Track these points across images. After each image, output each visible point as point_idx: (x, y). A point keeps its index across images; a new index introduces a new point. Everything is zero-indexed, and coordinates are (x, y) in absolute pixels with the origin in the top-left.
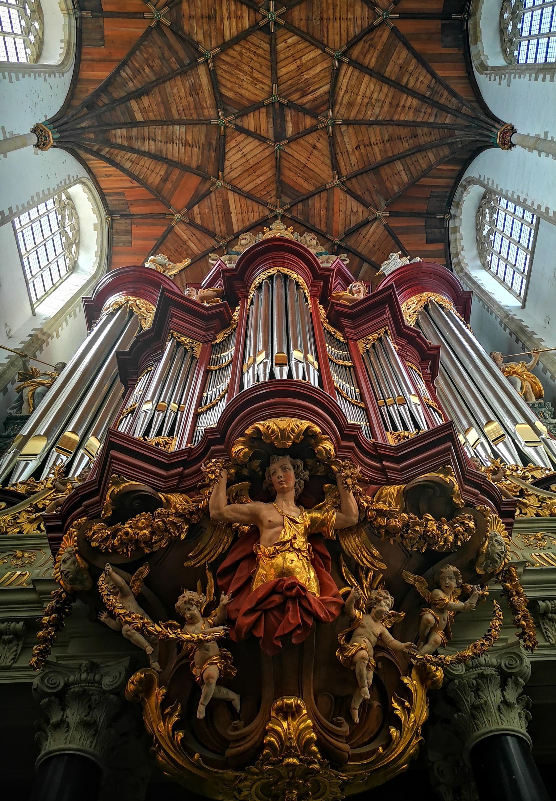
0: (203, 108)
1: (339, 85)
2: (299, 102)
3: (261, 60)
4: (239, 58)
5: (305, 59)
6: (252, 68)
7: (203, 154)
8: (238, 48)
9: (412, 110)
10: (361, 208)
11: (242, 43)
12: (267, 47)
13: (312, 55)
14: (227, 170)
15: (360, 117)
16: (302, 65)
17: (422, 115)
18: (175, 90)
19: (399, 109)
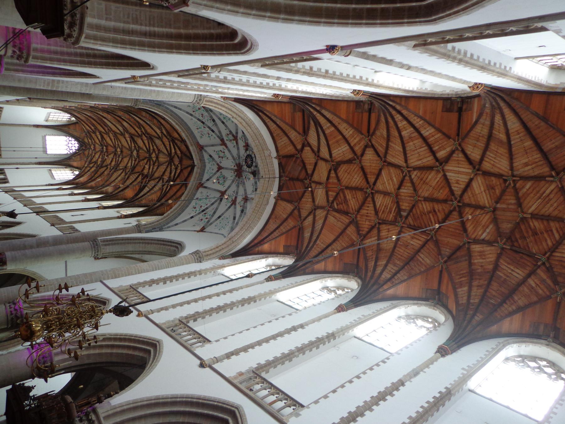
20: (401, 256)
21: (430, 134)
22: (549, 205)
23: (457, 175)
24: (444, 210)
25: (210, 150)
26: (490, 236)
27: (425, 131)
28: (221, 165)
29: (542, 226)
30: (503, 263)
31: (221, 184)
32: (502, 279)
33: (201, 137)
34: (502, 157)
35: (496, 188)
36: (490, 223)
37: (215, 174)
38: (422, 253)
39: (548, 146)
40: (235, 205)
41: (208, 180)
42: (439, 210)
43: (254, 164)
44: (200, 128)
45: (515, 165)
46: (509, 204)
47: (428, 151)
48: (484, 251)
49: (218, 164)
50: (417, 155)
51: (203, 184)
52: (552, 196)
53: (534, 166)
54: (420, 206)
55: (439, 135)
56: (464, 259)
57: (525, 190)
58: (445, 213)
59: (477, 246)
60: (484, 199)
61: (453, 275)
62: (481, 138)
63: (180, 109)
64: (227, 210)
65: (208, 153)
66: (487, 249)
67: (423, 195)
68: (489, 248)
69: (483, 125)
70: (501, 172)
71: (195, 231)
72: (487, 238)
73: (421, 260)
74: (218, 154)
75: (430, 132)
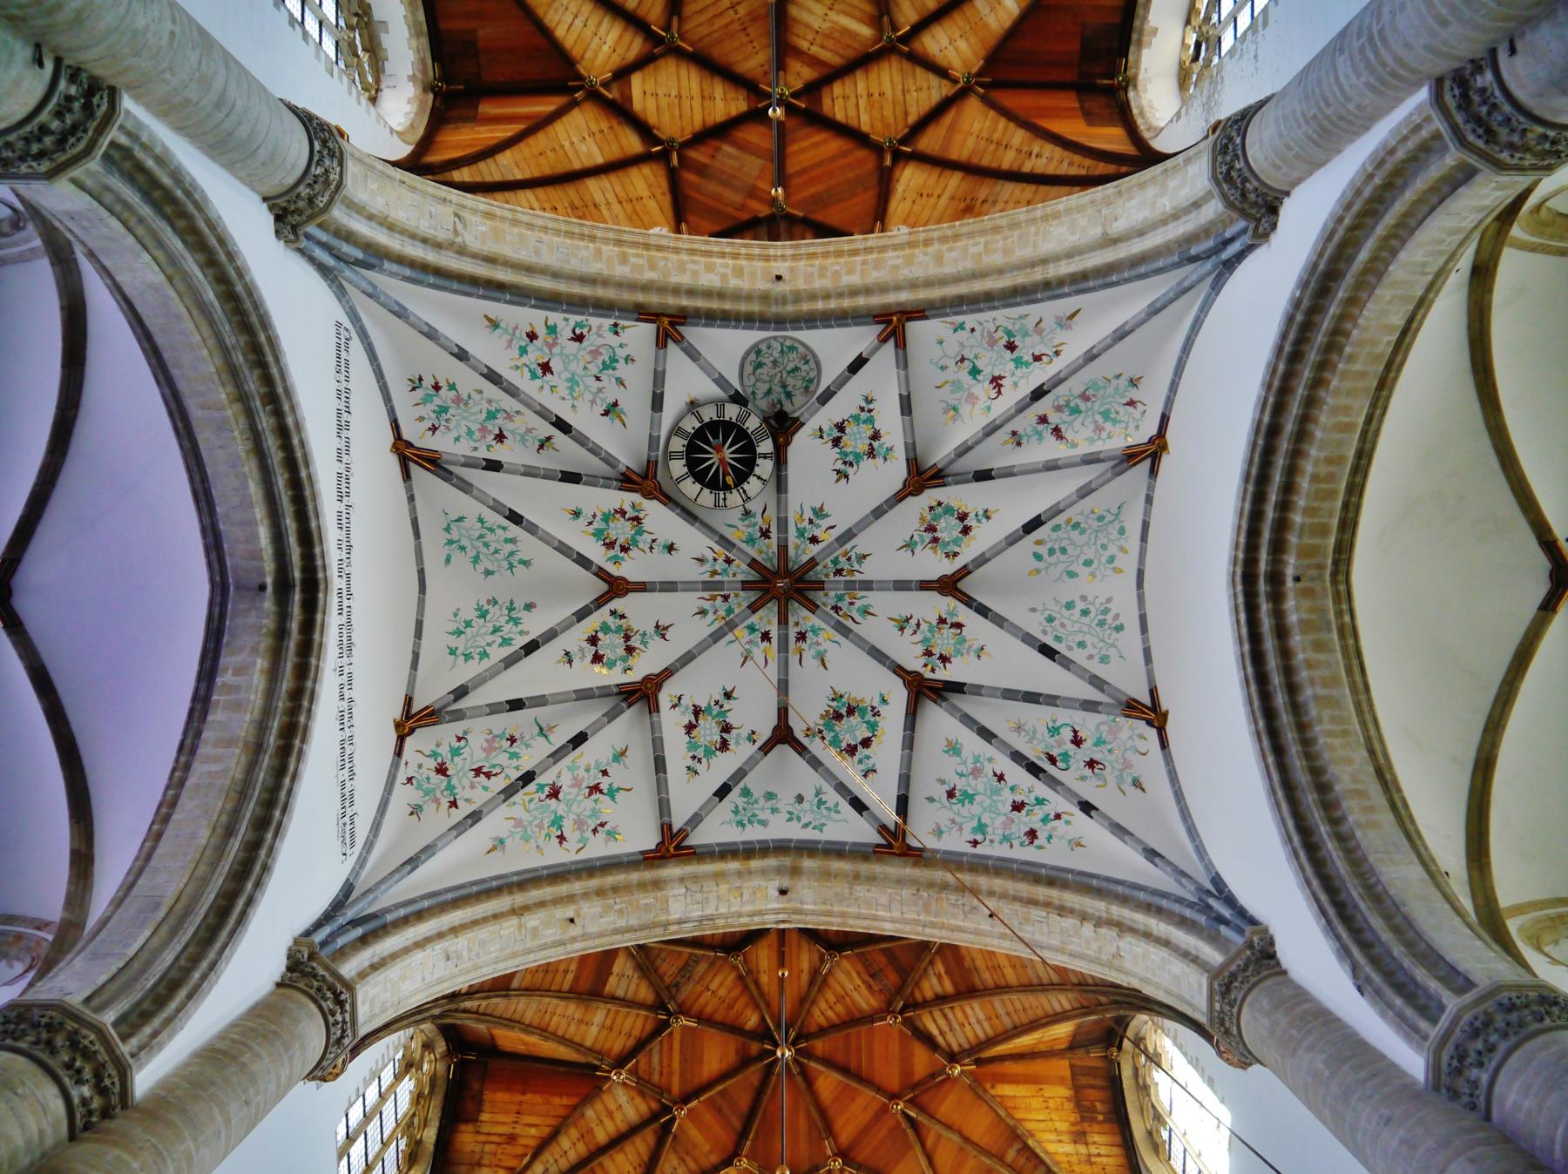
25: (687, 796)
28: (765, 733)
31: (873, 727)
33: (611, 835)
37: (815, 763)
40: (964, 572)
41: (859, 805)
43: (732, 412)
44: (557, 822)
49: (766, 748)
51: (882, 829)
63: (429, 850)
64: (999, 621)
65: (707, 808)
71: (1164, 744)
74: (709, 753)
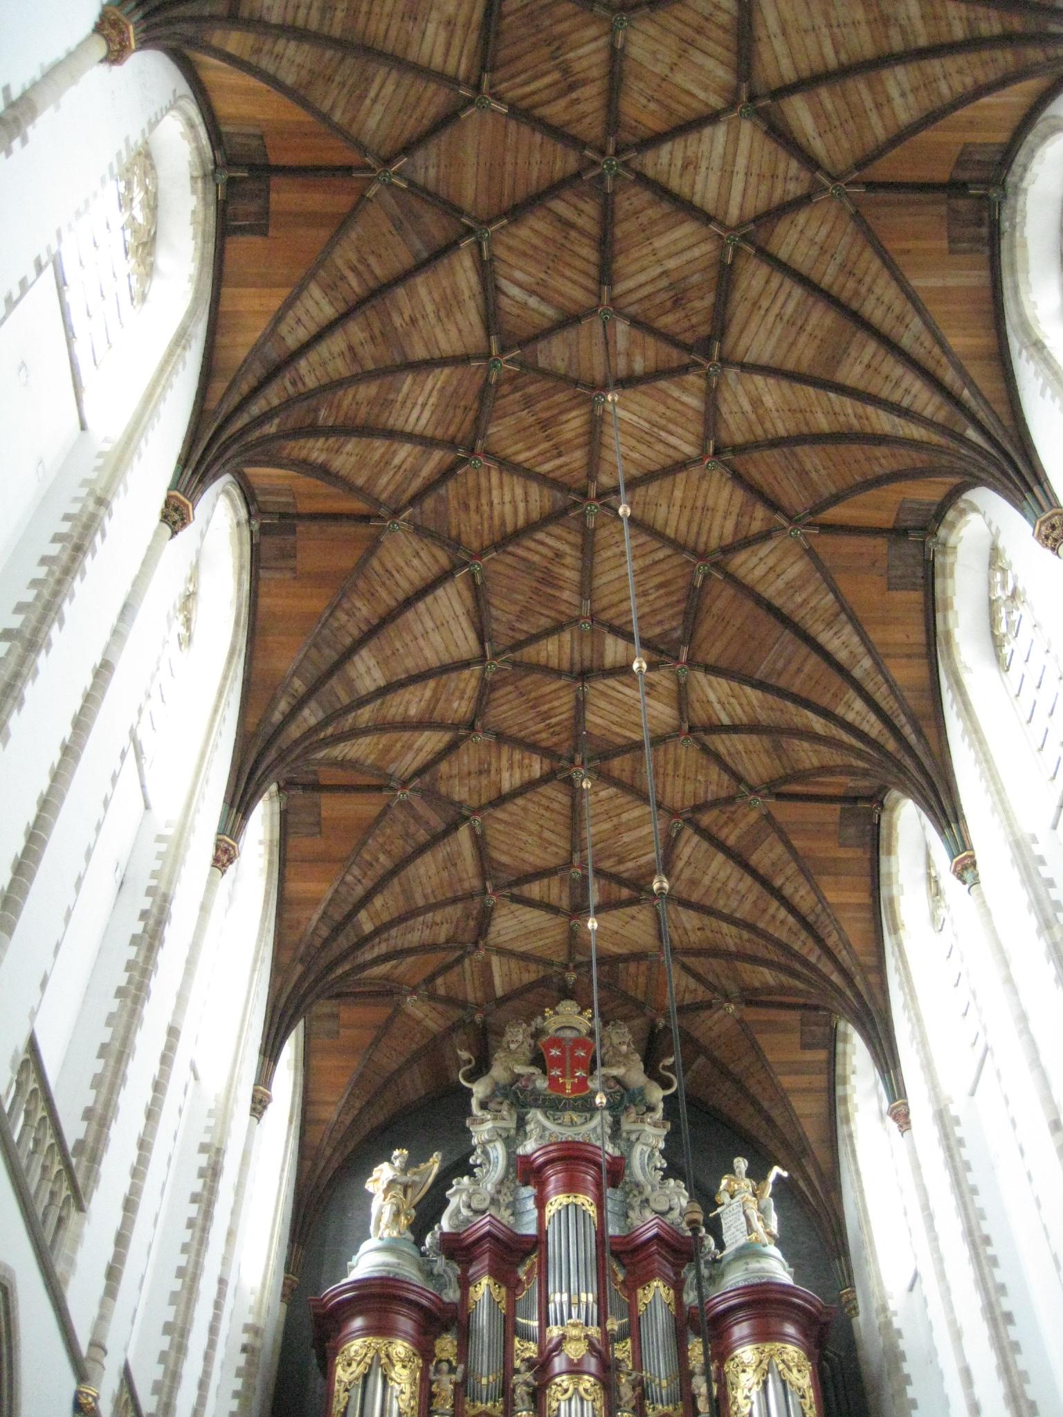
0: (461, 880)
1: (677, 851)
2: (614, 870)
3: (554, 816)
4: (522, 813)
5: (625, 817)
6: (542, 827)
7: (457, 927)
8: (520, 801)
9: (786, 928)
10: (701, 989)
11: (528, 795)
12: (566, 800)
13: (637, 813)
14: (491, 936)
15: (708, 903)
16: (620, 824)
17: (800, 943)
18: (422, 871)
19: (767, 917)
20: (369, 13)
21: (889, 100)
22: (633, 442)
23: (717, 162)
24: (579, 120)
26: (515, 311)
27: (907, 87)
29: (568, 436)
30: (441, 377)
32: (391, 397)
34: (785, 345)
35: (680, 314)
36: (559, 308)
38: (398, 85)
39: (811, 458)
42: (577, 101)
45: (759, 380)
46: (629, 355)
47: (818, 67)
48: (460, 304)
50: (805, 22)
52: (660, 447)
53: (753, 417)
54: (592, 31)
55: (881, 134)
56: (418, 245)
57: (676, 393)
58: (568, 123)
59: (473, 278)
60: (639, 275)
61: (353, 235)
62: (851, 284)
66: (471, 317)
67: (636, 38)
68: (475, 318)
69: (900, 318)
70: (734, 329)
72: (504, 302)
73: (372, 94)
75: (898, 102)
